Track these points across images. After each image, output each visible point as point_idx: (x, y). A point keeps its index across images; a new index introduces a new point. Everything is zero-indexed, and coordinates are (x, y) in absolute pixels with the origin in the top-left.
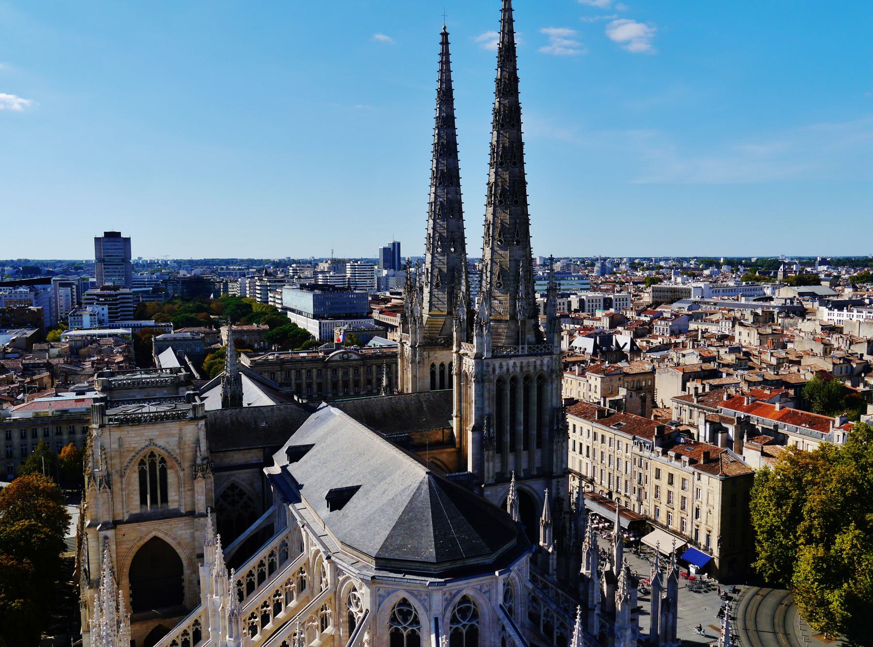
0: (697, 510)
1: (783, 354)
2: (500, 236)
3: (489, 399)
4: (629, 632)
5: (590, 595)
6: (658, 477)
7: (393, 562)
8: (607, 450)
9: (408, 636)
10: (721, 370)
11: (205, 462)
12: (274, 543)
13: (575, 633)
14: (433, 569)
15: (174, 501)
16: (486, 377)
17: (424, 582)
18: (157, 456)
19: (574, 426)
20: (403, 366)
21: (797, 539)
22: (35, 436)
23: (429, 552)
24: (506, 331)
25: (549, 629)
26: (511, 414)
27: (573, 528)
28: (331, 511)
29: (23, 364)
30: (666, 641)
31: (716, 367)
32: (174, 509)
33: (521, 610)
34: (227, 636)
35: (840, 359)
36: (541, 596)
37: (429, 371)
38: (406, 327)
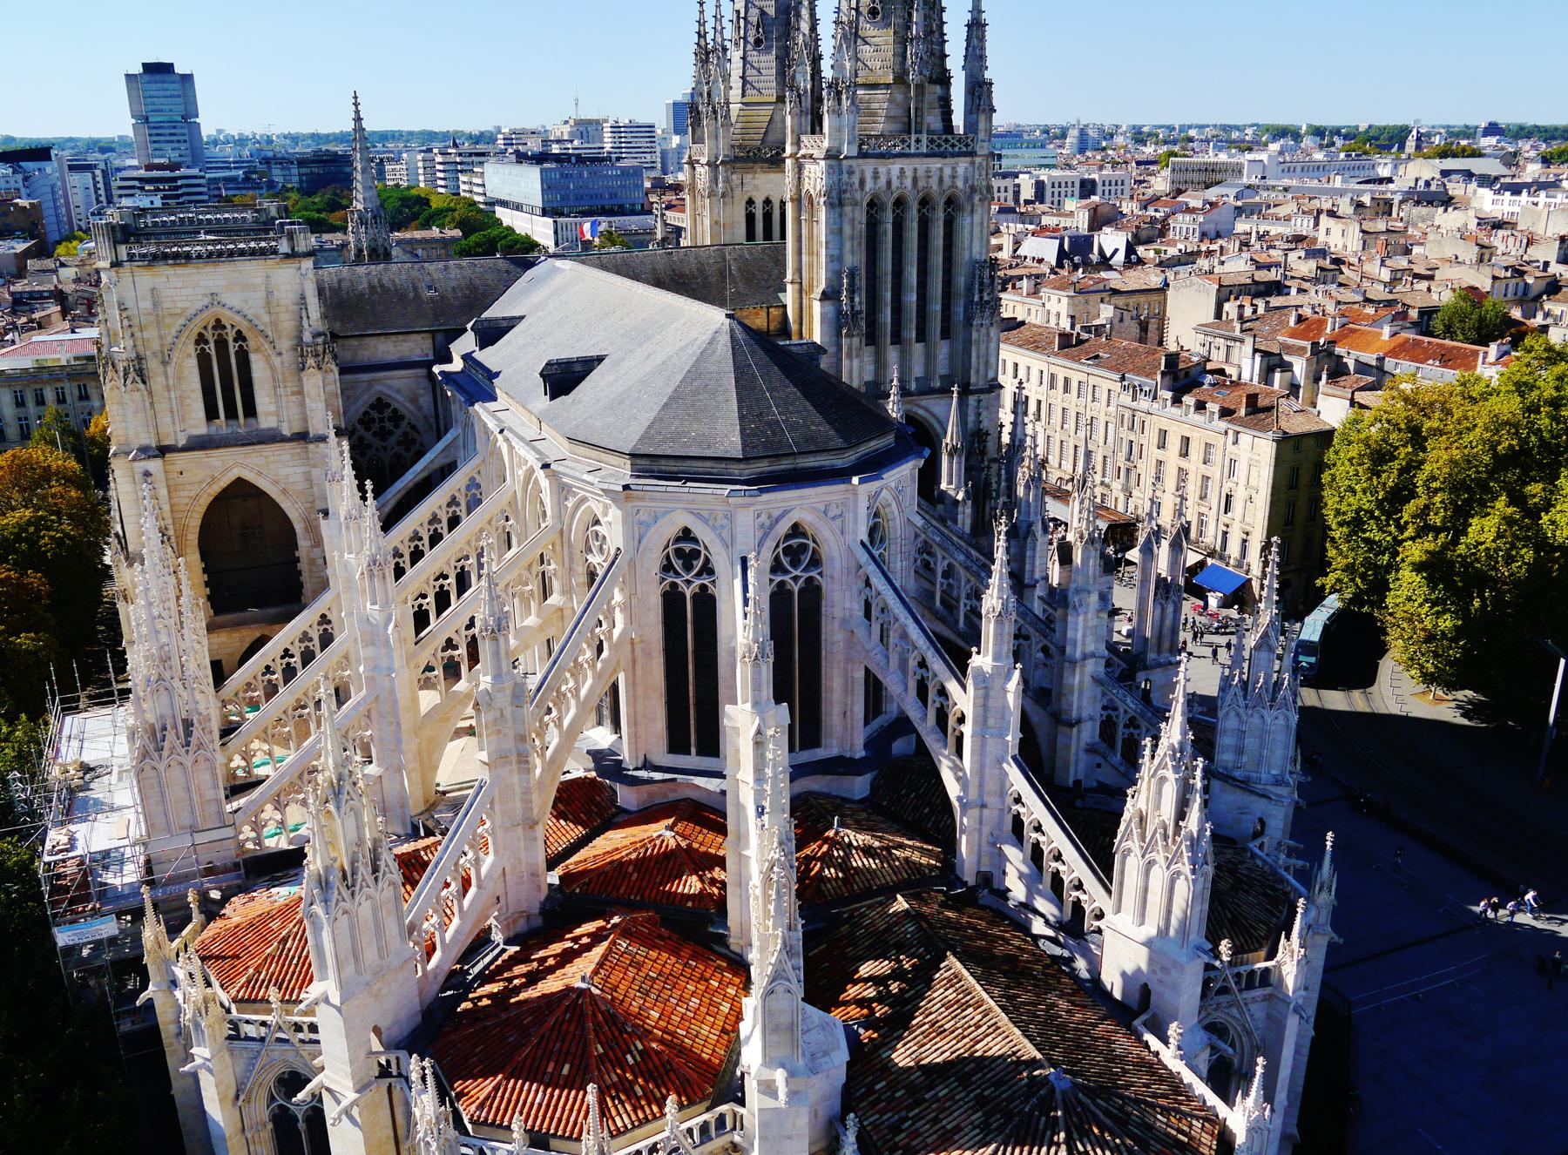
0: (1228, 497)
1: (1402, 262)
3: (852, 238)
5: (1027, 561)
6: (1162, 445)
7: (663, 462)
8: (1073, 404)
9: (695, 597)
10: (1287, 283)
11: (320, 340)
12: (454, 485)
13: (996, 568)
14: (736, 470)
15: (269, 414)
16: (848, 195)
17: (719, 492)
18: (229, 327)
19: (1016, 365)
21: (1402, 529)
22: (40, 401)
23: (731, 442)
24: (885, 105)
25: (950, 605)
27: (1003, 477)
28: (552, 398)
29: (12, 294)
30: (1159, 652)
31: (1279, 278)
32: (269, 429)
33: (901, 566)
35: (1506, 269)
36: (938, 539)
37: (743, 213)
38: (698, 132)
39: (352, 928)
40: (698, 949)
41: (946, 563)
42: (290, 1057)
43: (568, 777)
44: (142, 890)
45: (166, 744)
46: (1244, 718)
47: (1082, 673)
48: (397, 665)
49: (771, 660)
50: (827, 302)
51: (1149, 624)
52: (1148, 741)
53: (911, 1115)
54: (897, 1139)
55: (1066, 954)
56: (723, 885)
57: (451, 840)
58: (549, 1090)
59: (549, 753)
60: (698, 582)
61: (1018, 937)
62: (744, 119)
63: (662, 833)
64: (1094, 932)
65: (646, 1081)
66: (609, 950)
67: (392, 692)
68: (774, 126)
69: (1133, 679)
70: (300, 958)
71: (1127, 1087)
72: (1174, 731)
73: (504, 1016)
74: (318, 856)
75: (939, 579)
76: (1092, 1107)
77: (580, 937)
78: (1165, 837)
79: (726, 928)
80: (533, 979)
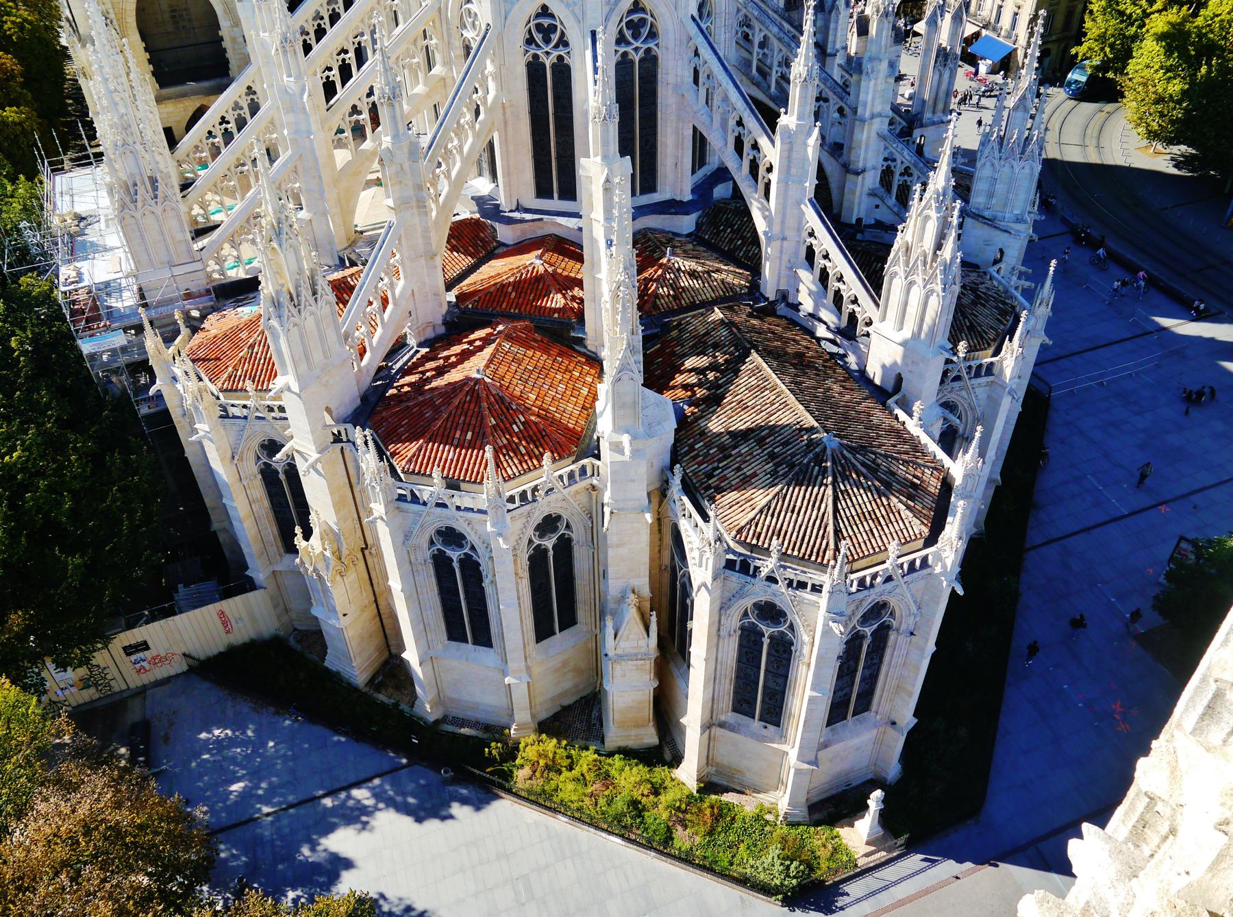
4: (884, 66)
5: (831, 32)
9: (553, 66)
25: (764, 73)
30: (934, 112)
33: (725, 37)
34: (285, 76)
39: (302, 336)
40: (564, 349)
41: (762, 35)
42: (268, 429)
43: (458, 218)
44: (139, 311)
45: (139, 197)
46: (998, 168)
47: (869, 130)
48: (314, 128)
49: (617, 120)
51: (928, 88)
52: (918, 187)
53: (721, 465)
54: (710, 482)
55: (841, 351)
56: (582, 300)
57: (370, 269)
58: (458, 450)
59: (441, 199)
60: (555, 53)
61: (805, 339)
63: (533, 261)
64: (863, 335)
65: (528, 443)
66: (497, 350)
67: (313, 151)
69: (911, 135)
70: (265, 359)
71: (880, 446)
72: (940, 179)
73: (421, 399)
74: (270, 283)
75: (756, 49)
76: (853, 461)
77: (474, 341)
78: (925, 263)
79: (585, 333)
80: (440, 372)
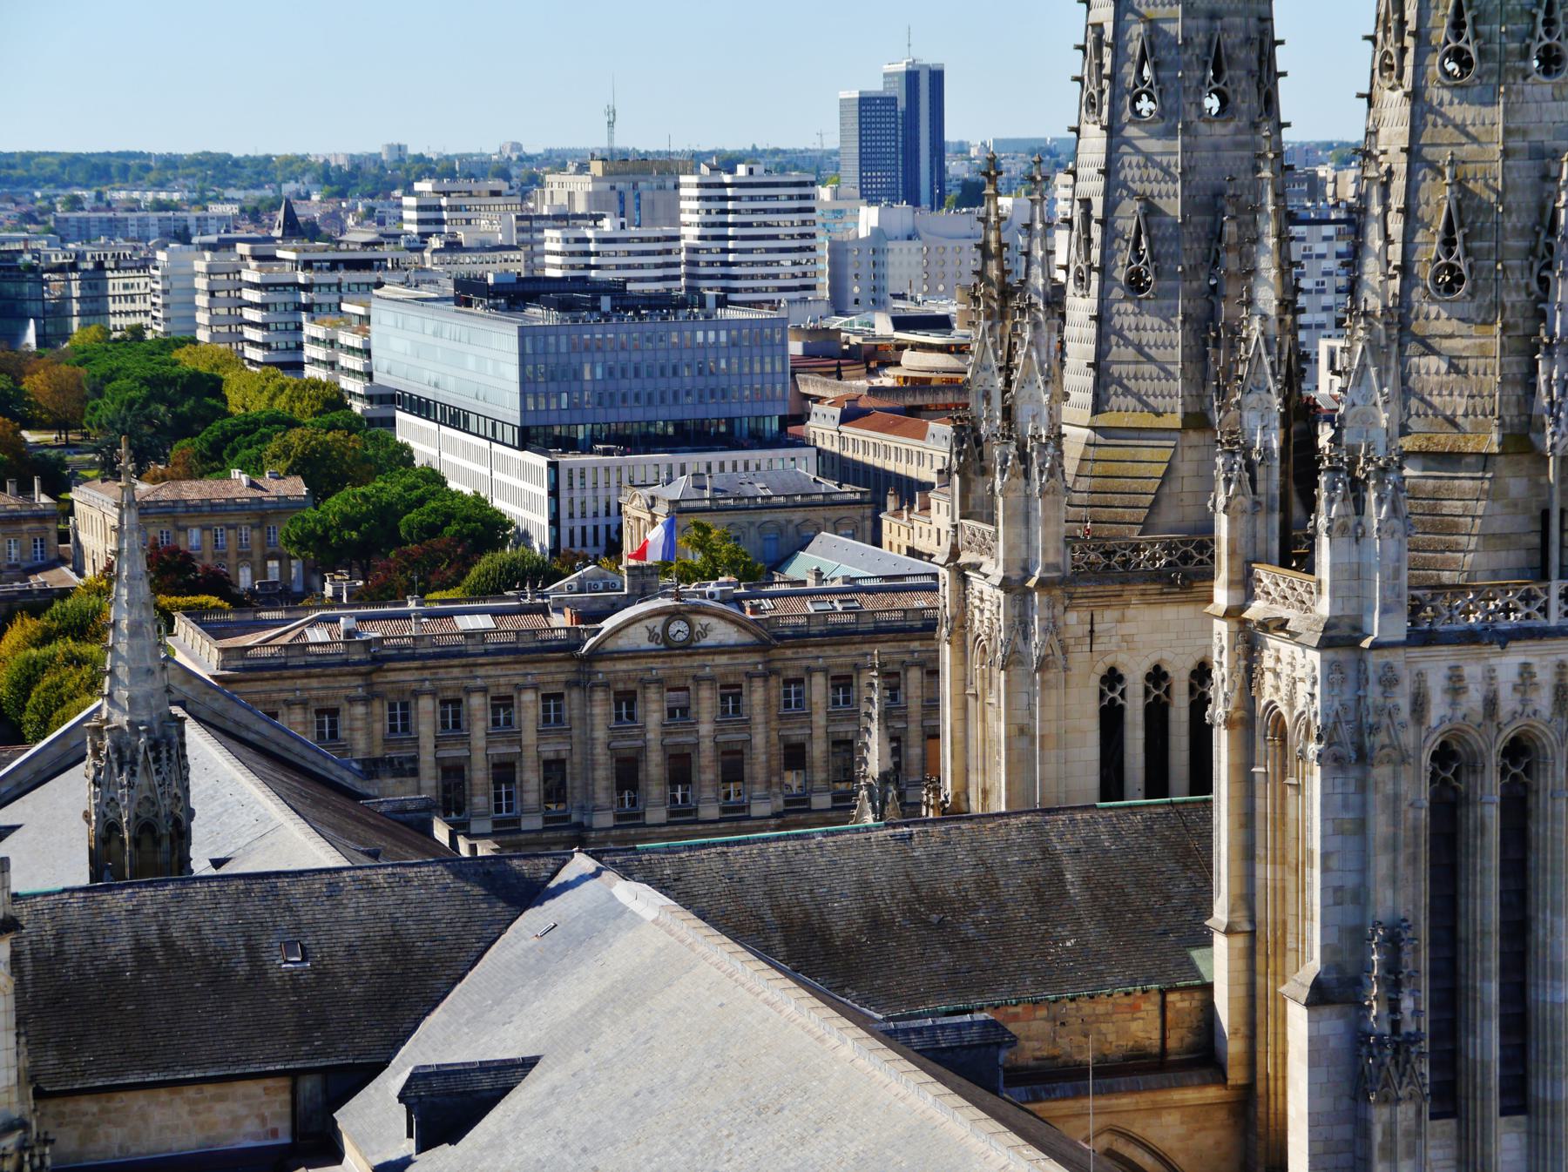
2: (1457, 26)
3: (1394, 848)
16: (1382, 738)
20: (964, 681)
26: (1504, 923)
37: (1092, 707)
38: (979, 488)
50: (1326, 1011)
62: (1099, 468)
68: (1175, 486)
